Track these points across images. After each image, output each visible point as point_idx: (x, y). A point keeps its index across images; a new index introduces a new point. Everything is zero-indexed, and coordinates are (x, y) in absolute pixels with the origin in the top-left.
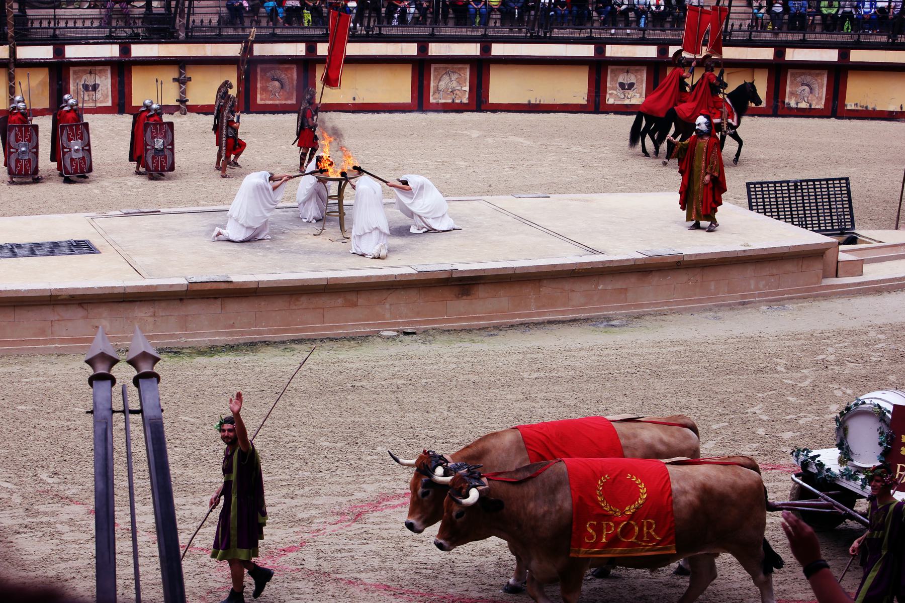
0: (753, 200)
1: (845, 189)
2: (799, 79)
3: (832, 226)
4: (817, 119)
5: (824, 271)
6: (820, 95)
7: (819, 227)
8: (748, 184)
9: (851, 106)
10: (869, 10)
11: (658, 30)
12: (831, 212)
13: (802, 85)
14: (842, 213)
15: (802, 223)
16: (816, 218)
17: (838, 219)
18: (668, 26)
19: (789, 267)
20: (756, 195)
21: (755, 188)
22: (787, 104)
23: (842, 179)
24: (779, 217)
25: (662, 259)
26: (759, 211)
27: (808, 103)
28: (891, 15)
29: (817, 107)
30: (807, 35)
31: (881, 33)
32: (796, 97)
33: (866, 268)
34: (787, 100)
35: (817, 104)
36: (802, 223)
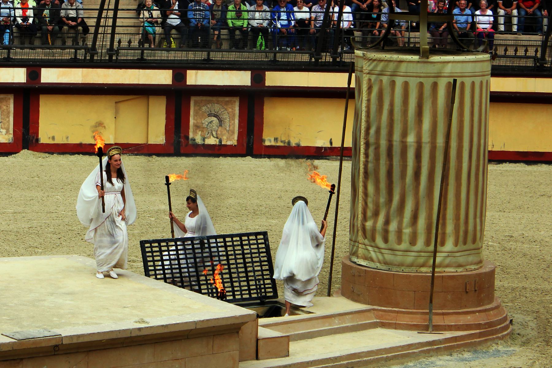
0: (150, 264)
1: (263, 246)
2: (204, 108)
3: (250, 294)
4: (229, 159)
5: (241, 352)
6: (231, 128)
7: (234, 295)
8: (142, 243)
9: (270, 141)
10: (285, 23)
11: (27, 48)
12: (247, 277)
13: (210, 115)
14: (260, 277)
15: (212, 290)
16: (229, 284)
17: (256, 285)
18: (37, 43)
19: (197, 347)
20: (153, 256)
21: (151, 247)
22: (192, 139)
23: (259, 234)
24: (183, 284)
25: (34, 343)
26: (158, 277)
27: (217, 138)
28: (312, 29)
29: (229, 143)
30: (212, 54)
31: (301, 51)
32: (202, 131)
33: (293, 346)
34: (191, 135)
35: (228, 139)
36: (212, 290)
